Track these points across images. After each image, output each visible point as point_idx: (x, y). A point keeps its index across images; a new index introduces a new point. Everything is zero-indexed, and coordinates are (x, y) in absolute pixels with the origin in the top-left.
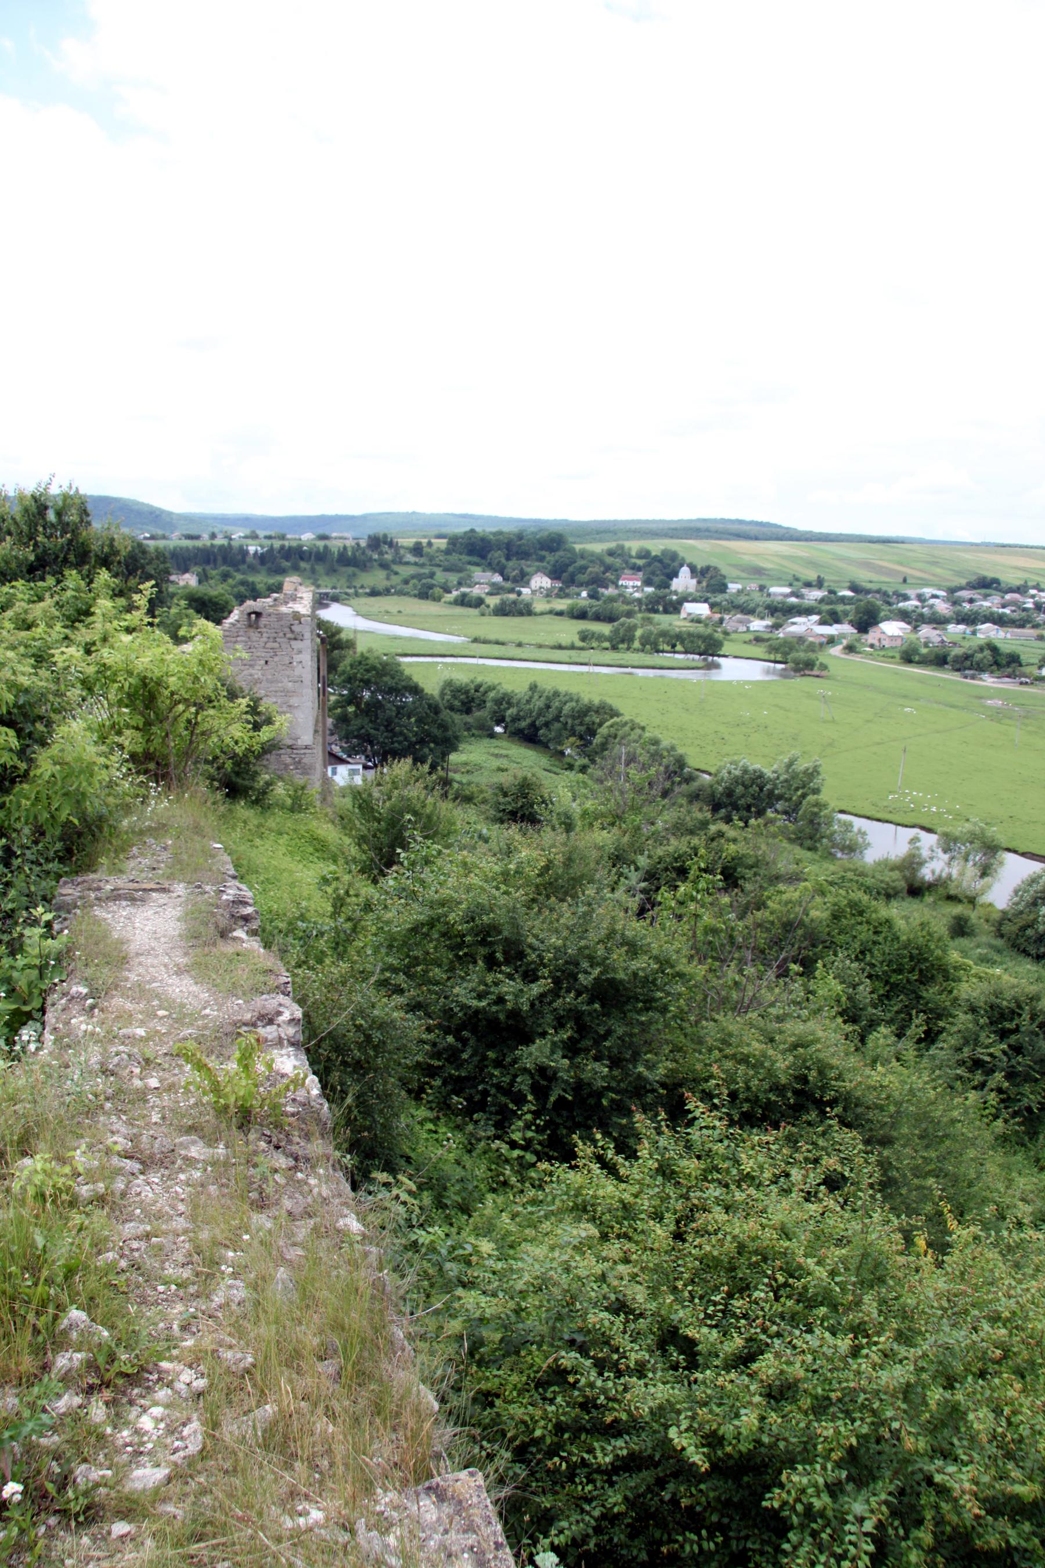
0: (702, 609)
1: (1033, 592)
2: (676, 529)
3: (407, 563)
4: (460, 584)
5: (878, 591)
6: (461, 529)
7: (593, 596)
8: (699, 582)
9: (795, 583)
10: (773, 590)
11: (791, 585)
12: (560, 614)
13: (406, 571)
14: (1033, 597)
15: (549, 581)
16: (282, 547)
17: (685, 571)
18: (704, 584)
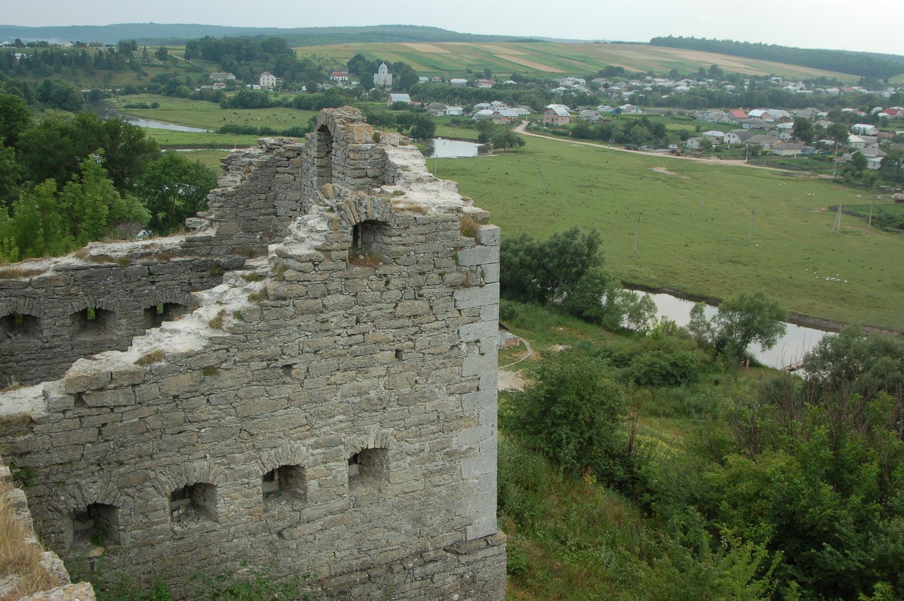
0: (405, 98)
1: (649, 78)
2: (366, 34)
3: (156, 66)
4: (200, 83)
5: (534, 80)
6: (196, 36)
7: (311, 90)
8: (394, 77)
9: (469, 75)
10: (452, 81)
11: (465, 78)
12: (289, 106)
13: (153, 73)
14: (650, 82)
15: (275, 78)
16: (45, 53)
17: (383, 68)
18: (399, 77)
